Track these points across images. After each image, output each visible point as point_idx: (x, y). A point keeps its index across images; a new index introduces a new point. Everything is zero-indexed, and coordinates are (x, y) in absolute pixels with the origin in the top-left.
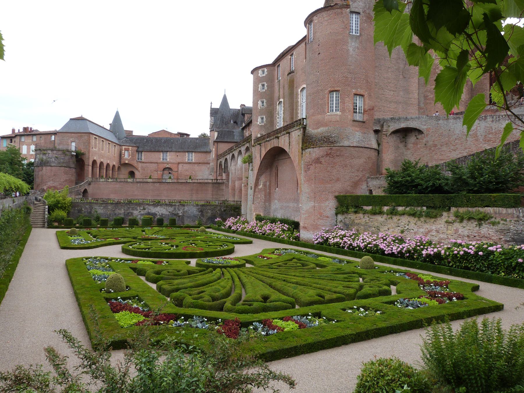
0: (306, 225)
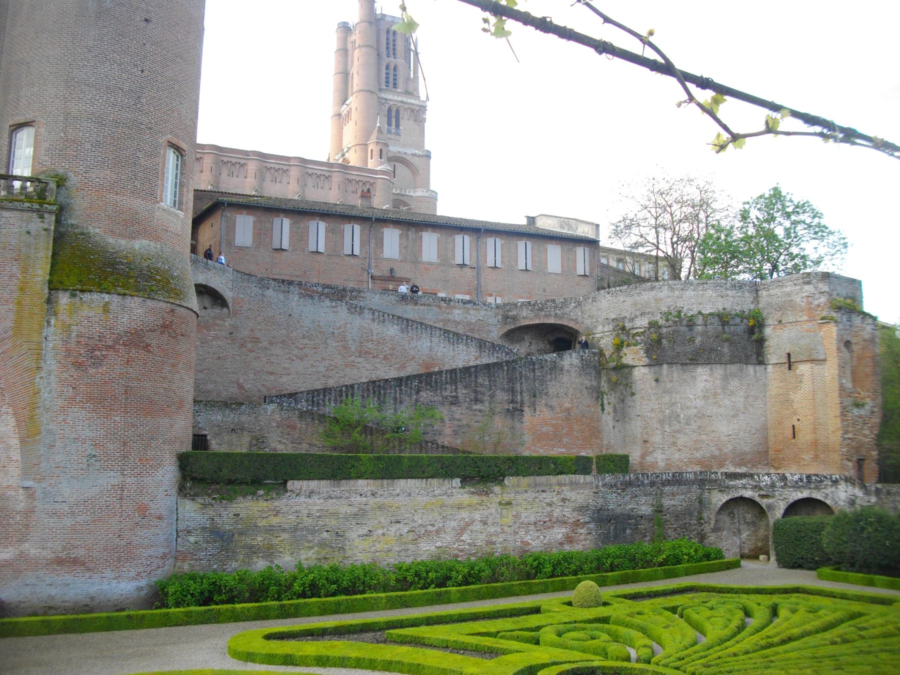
0: (80, 553)
